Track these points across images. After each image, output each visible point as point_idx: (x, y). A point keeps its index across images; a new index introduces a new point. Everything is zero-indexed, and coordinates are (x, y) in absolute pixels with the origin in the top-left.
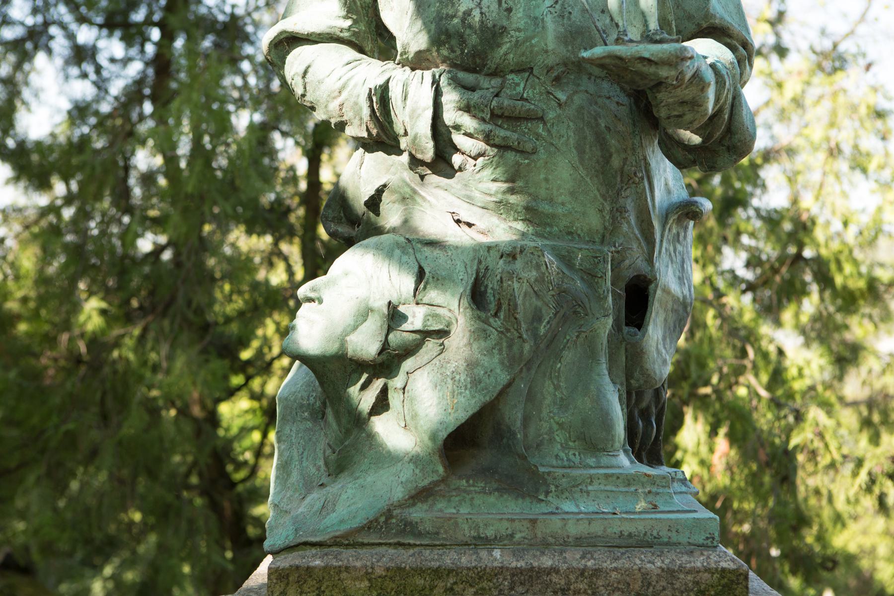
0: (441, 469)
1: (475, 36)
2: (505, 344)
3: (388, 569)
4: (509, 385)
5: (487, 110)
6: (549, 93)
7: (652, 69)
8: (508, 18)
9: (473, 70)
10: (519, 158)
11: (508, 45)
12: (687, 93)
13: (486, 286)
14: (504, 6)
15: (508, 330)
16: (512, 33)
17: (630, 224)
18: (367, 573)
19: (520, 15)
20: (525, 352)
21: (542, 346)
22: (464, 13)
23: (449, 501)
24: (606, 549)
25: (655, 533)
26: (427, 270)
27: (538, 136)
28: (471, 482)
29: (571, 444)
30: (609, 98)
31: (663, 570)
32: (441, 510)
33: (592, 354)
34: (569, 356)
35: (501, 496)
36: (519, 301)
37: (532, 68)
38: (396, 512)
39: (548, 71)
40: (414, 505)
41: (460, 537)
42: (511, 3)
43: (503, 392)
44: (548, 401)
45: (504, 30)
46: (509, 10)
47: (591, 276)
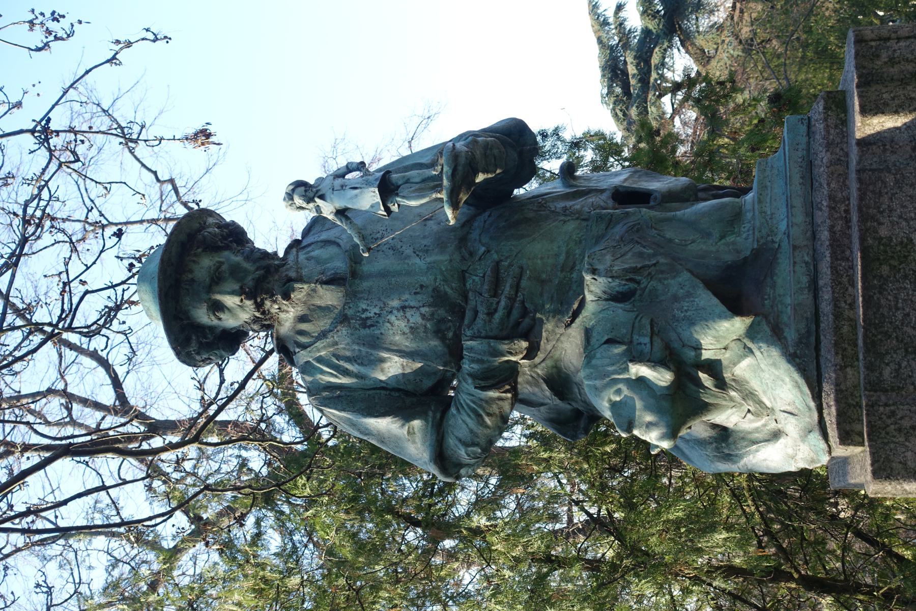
1: (439, 312)
2: (660, 276)
3: (837, 353)
5: (491, 300)
6: (480, 259)
7: (460, 168)
8: (427, 287)
9: (464, 313)
10: (525, 278)
11: (446, 287)
13: (618, 292)
14: (419, 290)
15: (650, 274)
16: (437, 284)
17: (577, 204)
18: (841, 369)
19: (425, 279)
20: (666, 261)
22: (423, 319)
23: (782, 312)
24: (814, 194)
25: (800, 160)
26: (606, 338)
27: (510, 265)
28: (766, 297)
29: (736, 230)
30: (485, 221)
31: (827, 151)
32: (789, 318)
34: (669, 234)
35: (776, 274)
36: (626, 266)
37: (463, 271)
38: (791, 350)
39: (465, 260)
40: (785, 338)
43: (697, 276)
44: (704, 247)
45: (435, 290)
46: (422, 286)
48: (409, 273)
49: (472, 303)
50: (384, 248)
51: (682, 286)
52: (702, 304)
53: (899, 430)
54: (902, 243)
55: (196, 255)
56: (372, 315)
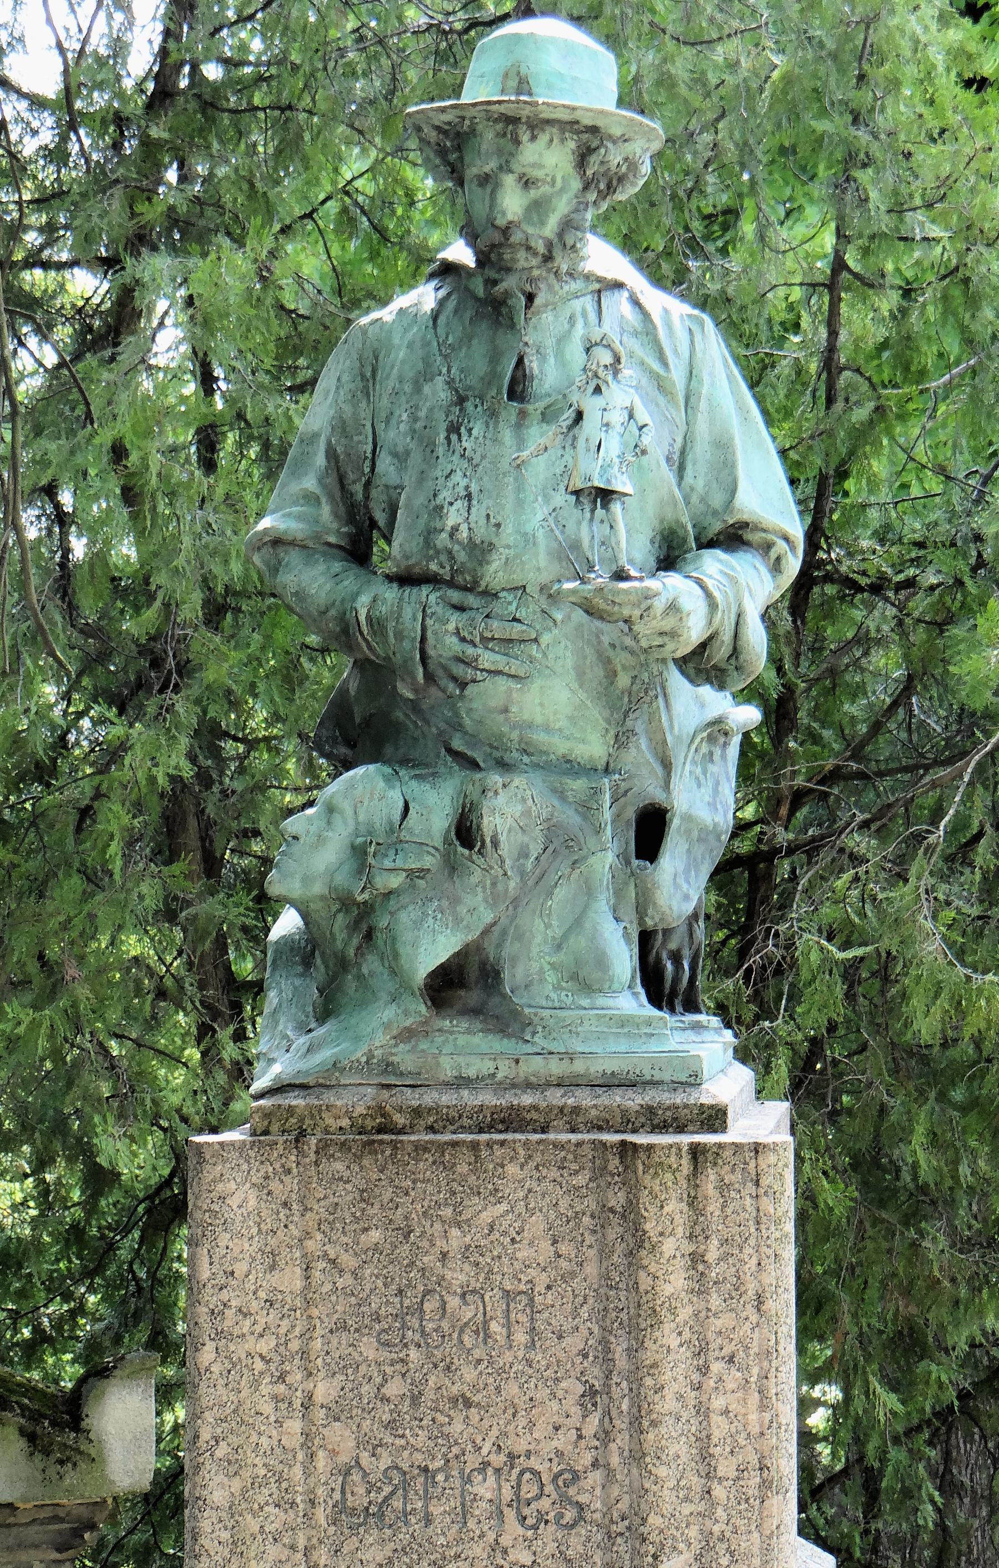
0: (423, 1009)
4: (494, 924)
8: (497, 534)
12: (668, 624)
14: (493, 521)
21: (530, 883)
27: (532, 660)
33: (589, 891)
41: (442, 1077)
42: (499, 519)
43: (486, 932)
44: (538, 939)
46: (498, 525)
47: (587, 808)
48: (520, 503)
49: (471, 600)
50: (568, 457)
51: (471, 911)
52: (441, 939)
53: (266, 1178)
54: (496, 1190)
55: (563, 140)
56: (465, 444)
